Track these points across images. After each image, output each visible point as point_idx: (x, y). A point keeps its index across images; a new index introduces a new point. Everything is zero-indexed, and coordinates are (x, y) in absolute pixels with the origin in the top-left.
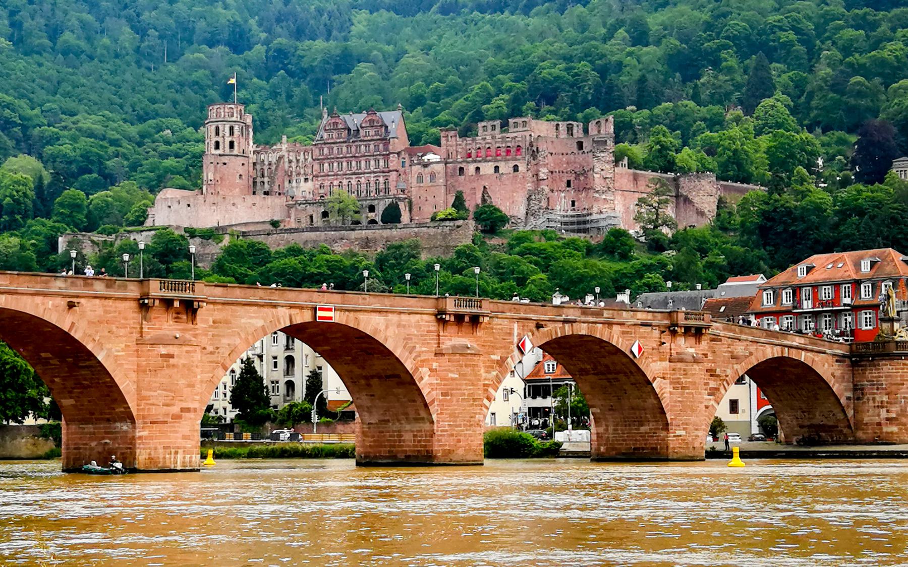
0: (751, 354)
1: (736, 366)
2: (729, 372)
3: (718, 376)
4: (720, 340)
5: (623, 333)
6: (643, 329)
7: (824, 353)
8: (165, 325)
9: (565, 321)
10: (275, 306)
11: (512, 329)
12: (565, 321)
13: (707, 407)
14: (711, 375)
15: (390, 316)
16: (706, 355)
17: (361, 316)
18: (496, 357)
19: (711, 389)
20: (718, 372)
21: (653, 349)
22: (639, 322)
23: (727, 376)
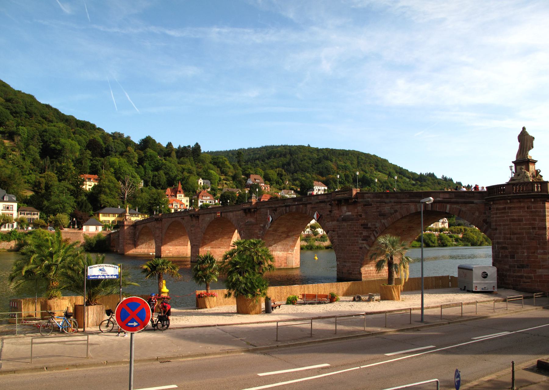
0: (396, 211)
1: (383, 221)
2: (378, 225)
3: (370, 228)
4: (371, 205)
5: (312, 208)
6: (322, 205)
7: (472, 203)
8: (195, 222)
9: (286, 206)
10: (211, 213)
11: (267, 213)
12: (286, 206)
13: (361, 248)
14: (364, 228)
15: (235, 213)
16: (361, 216)
17: (228, 214)
18: (262, 225)
19: (364, 236)
20: (369, 225)
21: (328, 215)
22: (318, 201)
23: (376, 228)
